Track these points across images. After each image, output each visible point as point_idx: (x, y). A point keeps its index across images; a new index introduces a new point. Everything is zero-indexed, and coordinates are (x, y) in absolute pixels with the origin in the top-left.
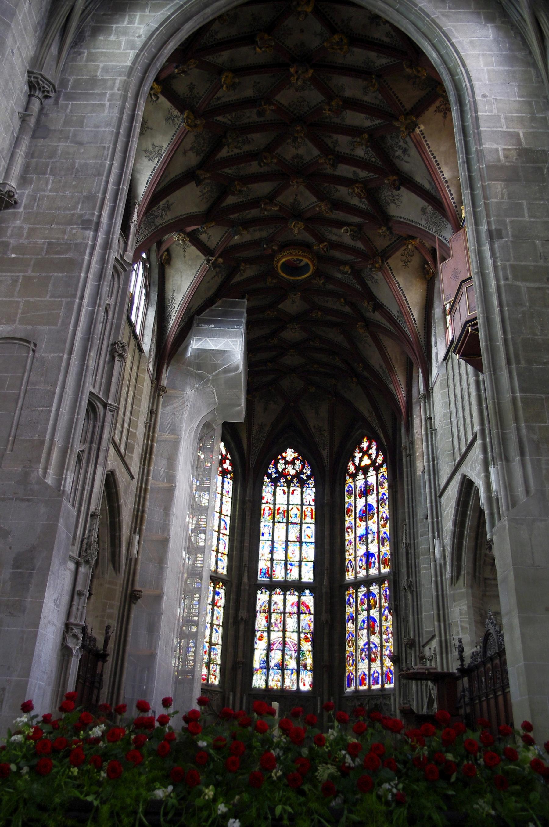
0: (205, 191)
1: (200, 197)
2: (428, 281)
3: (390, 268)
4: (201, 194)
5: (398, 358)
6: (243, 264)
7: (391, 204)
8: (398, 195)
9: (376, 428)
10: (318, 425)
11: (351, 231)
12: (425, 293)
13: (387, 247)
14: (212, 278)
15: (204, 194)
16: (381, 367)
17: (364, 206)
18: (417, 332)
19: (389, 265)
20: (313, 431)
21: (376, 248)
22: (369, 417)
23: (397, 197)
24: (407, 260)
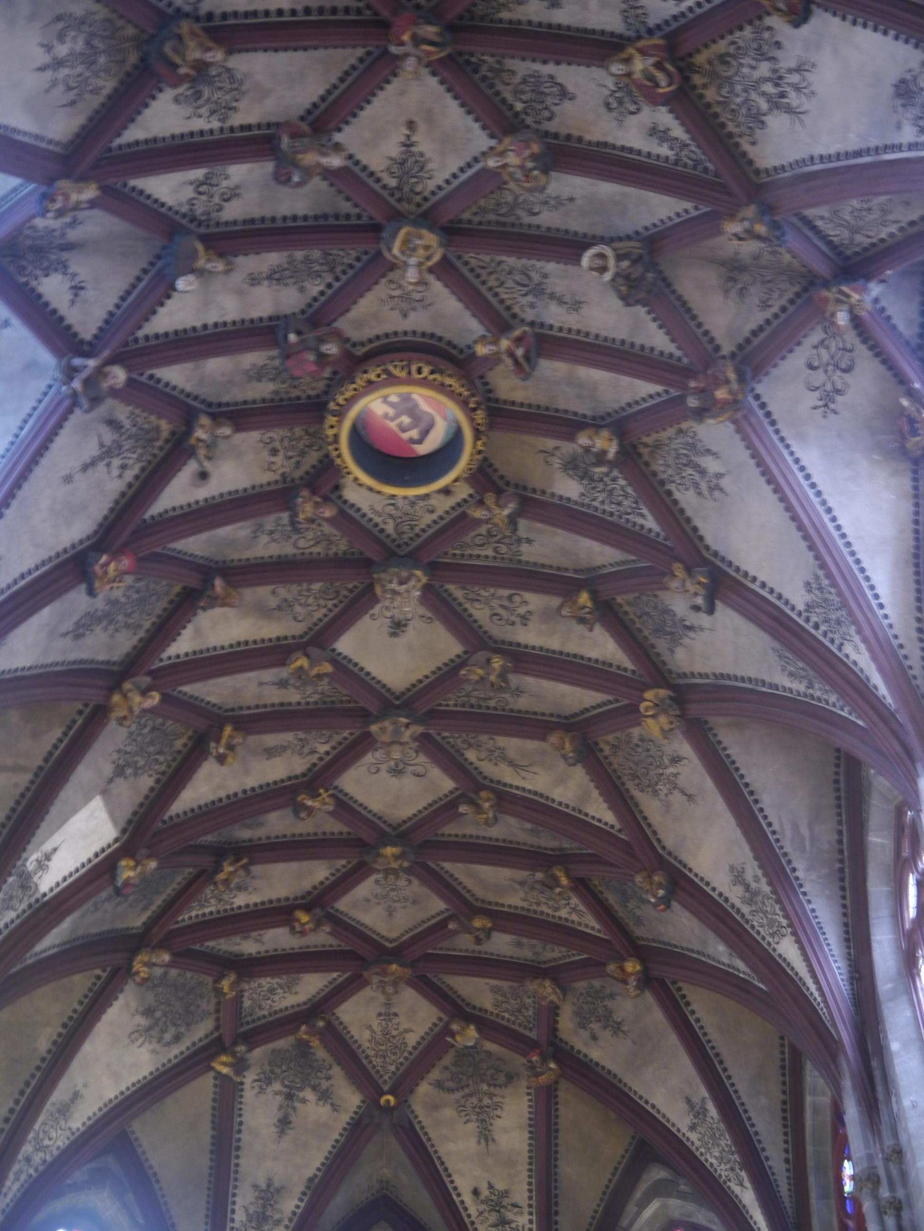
0: (62, 50)
1: (42, 69)
2: (916, 462)
3: (768, 414)
4: (46, 59)
5: (805, 831)
6: (205, 420)
7: (769, 119)
8: (798, 70)
9: (722, 1171)
10: (491, 1187)
11: (619, 258)
12: (907, 507)
13: (755, 333)
14: (85, 468)
15: (58, 63)
16: (738, 877)
17: (664, 150)
18: (895, 643)
19: (763, 406)
20: (473, 1211)
21: (712, 340)
22: (693, 1128)
23: (794, 78)
24: (829, 387)
